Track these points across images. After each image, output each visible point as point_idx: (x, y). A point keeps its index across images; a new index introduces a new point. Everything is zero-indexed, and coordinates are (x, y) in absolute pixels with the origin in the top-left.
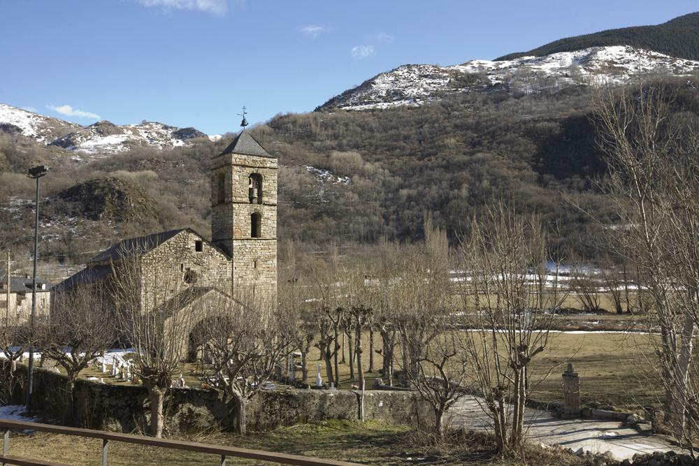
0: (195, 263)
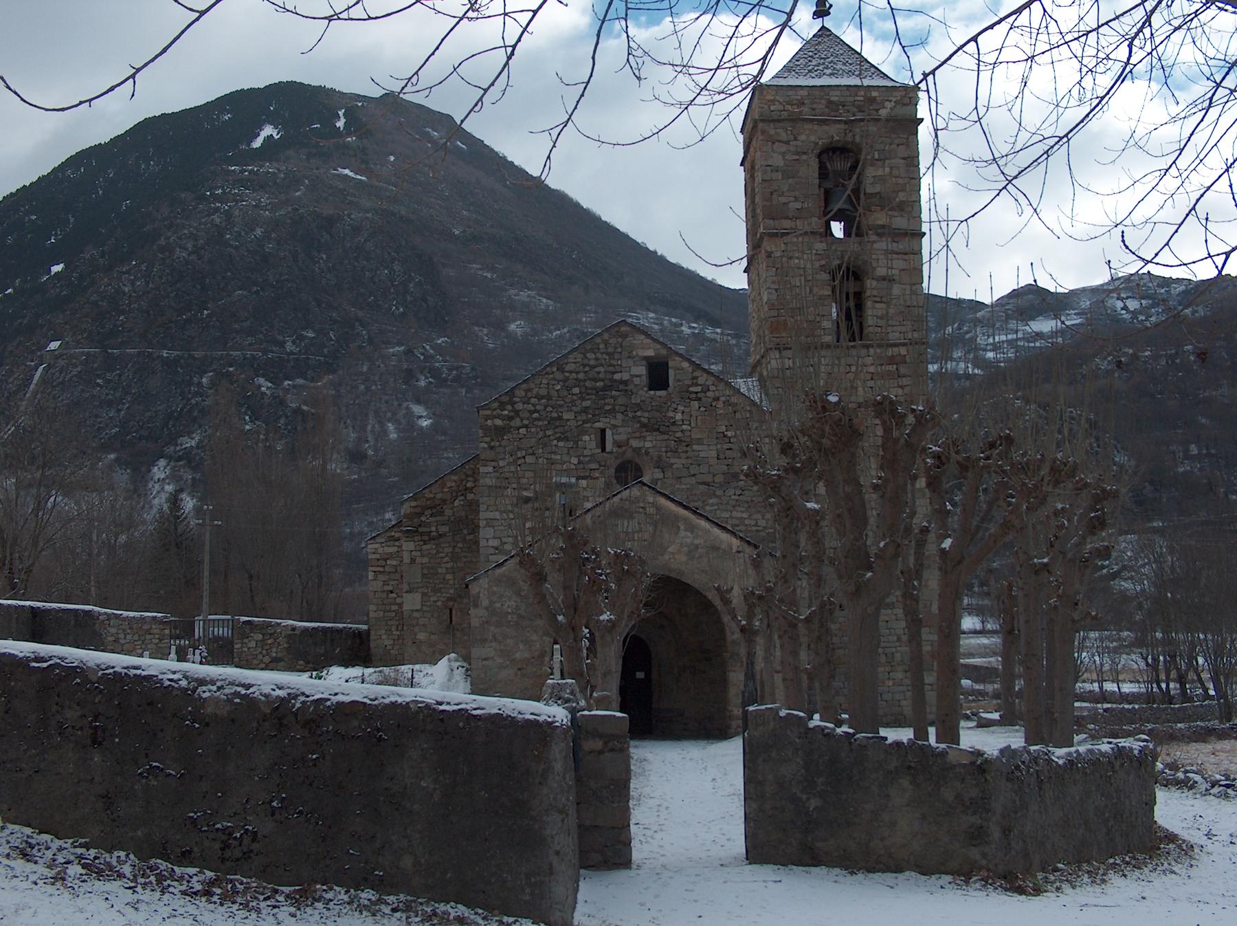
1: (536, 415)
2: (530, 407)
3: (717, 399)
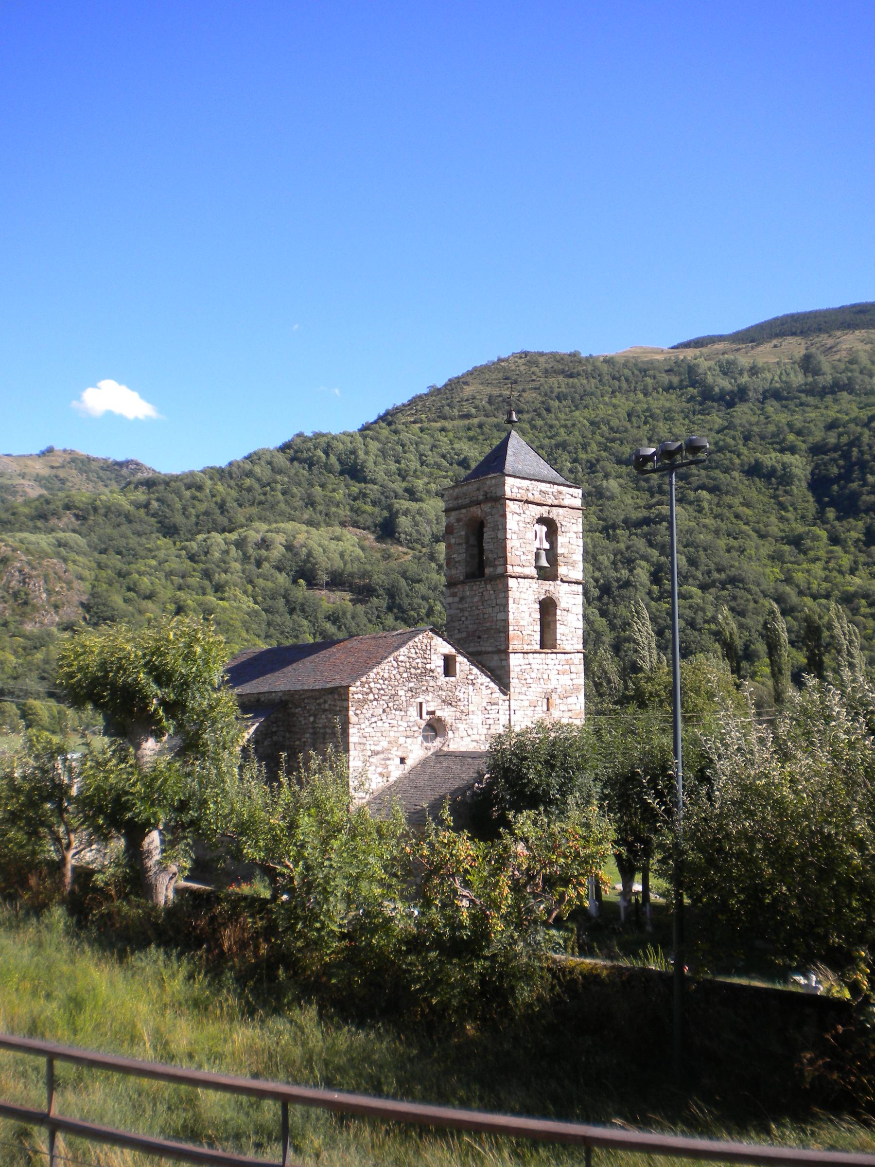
0: (444, 701)
1: (382, 692)
2: (379, 686)
3: (482, 684)
